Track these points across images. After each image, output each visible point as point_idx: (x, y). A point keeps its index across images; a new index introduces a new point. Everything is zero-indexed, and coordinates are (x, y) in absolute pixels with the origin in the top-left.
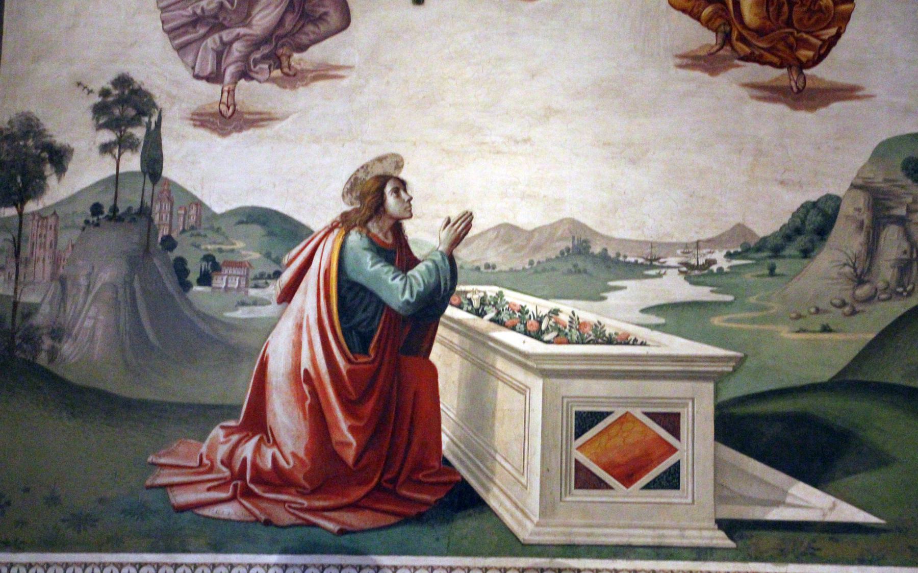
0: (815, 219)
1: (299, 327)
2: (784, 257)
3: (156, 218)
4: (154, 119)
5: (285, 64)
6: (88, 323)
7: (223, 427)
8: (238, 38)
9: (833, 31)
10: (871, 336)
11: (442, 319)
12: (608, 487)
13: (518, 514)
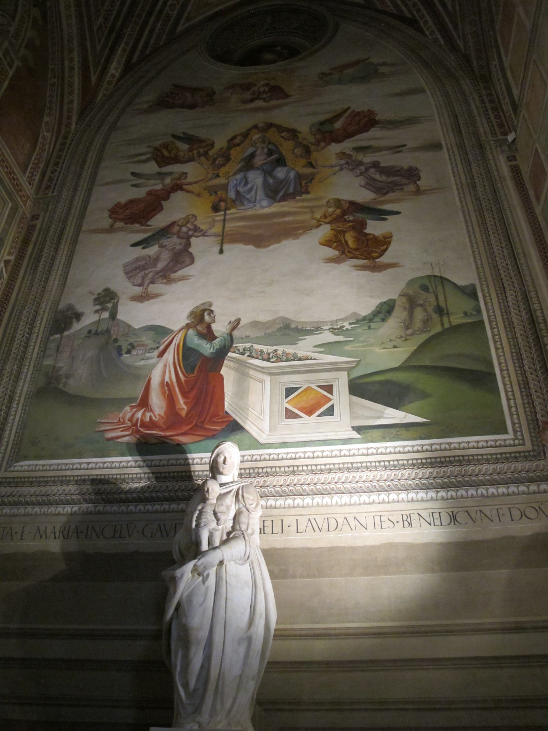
0: (385, 308)
1: (165, 366)
2: (374, 322)
3: (112, 332)
4: (116, 300)
5: (168, 277)
6: (80, 372)
7: (130, 406)
8: (151, 272)
9: (385, 247)
10: (415, 348)
11: (226, 358)
12: (301, 417)
13: (259, 431)
